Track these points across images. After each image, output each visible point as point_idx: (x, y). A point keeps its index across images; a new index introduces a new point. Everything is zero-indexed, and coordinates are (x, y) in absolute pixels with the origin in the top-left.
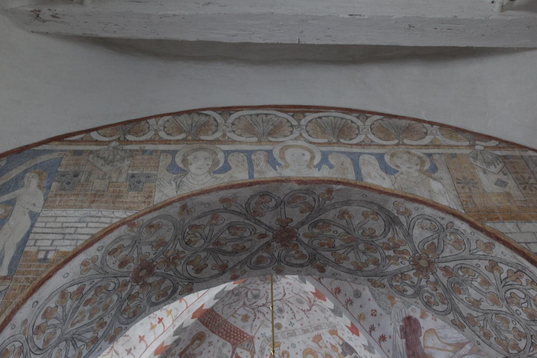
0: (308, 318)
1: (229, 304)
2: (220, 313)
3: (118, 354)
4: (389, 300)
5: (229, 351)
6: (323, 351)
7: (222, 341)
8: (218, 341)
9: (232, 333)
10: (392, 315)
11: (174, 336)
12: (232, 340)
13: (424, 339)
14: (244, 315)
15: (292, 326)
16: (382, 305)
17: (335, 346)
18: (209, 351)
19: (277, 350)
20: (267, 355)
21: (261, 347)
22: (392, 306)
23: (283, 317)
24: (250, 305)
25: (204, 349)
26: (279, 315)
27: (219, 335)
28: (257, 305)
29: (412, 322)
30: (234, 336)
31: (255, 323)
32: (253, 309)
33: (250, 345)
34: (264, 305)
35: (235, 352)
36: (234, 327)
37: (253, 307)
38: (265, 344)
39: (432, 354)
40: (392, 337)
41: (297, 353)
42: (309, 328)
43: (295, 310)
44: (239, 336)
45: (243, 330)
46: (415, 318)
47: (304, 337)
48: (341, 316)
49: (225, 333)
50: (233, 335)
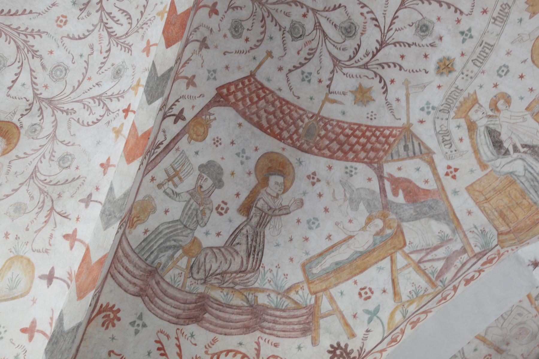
1: (296, 68)
2: (286, 95)
3: (66, 217)
5: (370, 180)
7: (339, 166)
8: (330, 168)
9: (353, 140)
11: (150, 102)
14: (354, 89)
15: (471, 37)
18: (320, 195)
19: (476, 111)
20: (461, 140)
21: (437, 133)
23: (441, 38)
24: (351, 59)
25: (305, 193)
26: (428, 40)
27: (323, 155)
30: (364, 145)
31: (392, 96)
32: (365, 66)
33: (410, 147)
34: (382, 44)
35: (385, 175)
36: (350, 124)
37: (361, 63)
38: (444, 122)
44: (373, 139)
45: (374, 123)
49: (335, 146)
50: (358, 143)
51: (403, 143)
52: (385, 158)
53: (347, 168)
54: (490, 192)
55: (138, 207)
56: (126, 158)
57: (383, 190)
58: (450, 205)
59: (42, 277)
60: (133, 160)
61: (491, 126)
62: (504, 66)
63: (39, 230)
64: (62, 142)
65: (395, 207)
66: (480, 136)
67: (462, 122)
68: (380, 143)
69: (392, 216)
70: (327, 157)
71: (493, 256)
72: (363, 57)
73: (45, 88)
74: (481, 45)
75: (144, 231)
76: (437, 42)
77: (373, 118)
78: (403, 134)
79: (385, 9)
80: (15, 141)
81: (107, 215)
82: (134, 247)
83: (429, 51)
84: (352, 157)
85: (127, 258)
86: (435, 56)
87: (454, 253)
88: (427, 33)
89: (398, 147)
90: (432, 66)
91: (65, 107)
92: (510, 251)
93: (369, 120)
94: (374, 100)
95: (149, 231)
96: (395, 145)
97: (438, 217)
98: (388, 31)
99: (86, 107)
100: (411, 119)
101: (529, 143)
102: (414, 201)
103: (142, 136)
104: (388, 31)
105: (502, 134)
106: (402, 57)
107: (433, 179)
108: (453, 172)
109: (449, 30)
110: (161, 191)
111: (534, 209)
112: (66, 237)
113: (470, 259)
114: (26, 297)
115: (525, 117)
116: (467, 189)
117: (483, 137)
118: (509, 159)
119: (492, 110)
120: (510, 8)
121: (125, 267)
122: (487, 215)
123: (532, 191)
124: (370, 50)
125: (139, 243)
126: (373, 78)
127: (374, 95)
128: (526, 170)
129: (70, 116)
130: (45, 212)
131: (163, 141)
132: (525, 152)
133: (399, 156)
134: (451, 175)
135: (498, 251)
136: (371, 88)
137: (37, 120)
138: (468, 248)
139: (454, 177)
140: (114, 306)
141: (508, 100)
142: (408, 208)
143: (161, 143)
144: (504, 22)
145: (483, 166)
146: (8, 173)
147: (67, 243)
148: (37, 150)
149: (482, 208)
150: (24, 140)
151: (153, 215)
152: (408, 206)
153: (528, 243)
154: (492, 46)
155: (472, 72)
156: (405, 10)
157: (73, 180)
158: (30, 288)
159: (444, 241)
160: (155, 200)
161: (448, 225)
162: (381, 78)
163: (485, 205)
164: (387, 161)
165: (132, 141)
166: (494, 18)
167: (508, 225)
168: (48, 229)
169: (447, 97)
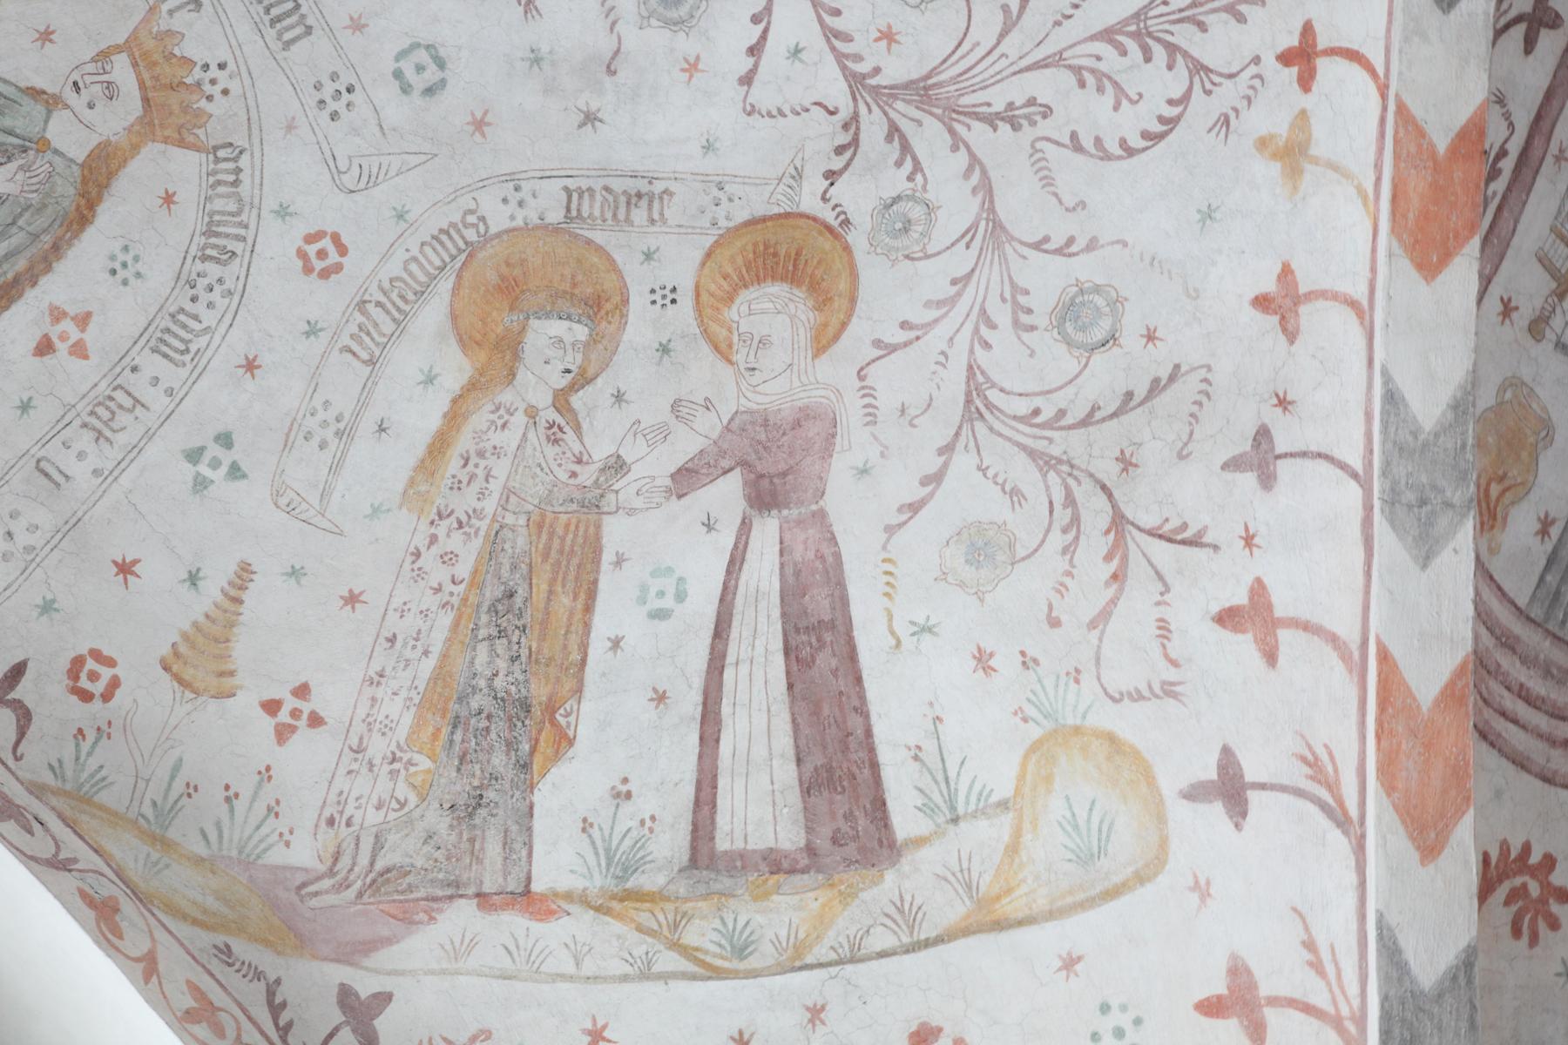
55: (1490, 440)
56: (1412, 260)
59: (1195, 793)
60: (1446, 257)
63: (1104, 615)
64: (1037, 246)
73: (884, 43)
75: (1538, 526)
80: (843, 285)
81: (1410, 507)
82: (1522, 601)
85: (1514, 650)
91: (998, 99)
95: (1553, 522)
99: (1090, 80)
103: (1453, 150)
110: (1547, 346)
112: (1228, 618)
114: (1163, 880)
121: (1516, 688)
125: (1535, 579)
129: (1028, 133)
130: (1095, 543)
131: (1506, 141)
137: (895, 181)
140: (1527, 849)
143: (1503, 153)
146: (871, 418)
147: (1243, 645)
148: (951, 301)
150: (873, 273)
151: (1550, 452)
157: (1156, 387)
158: (1164, 844)
160: (1538, 390)
165: (1418, 184)
168: (1139, 600)
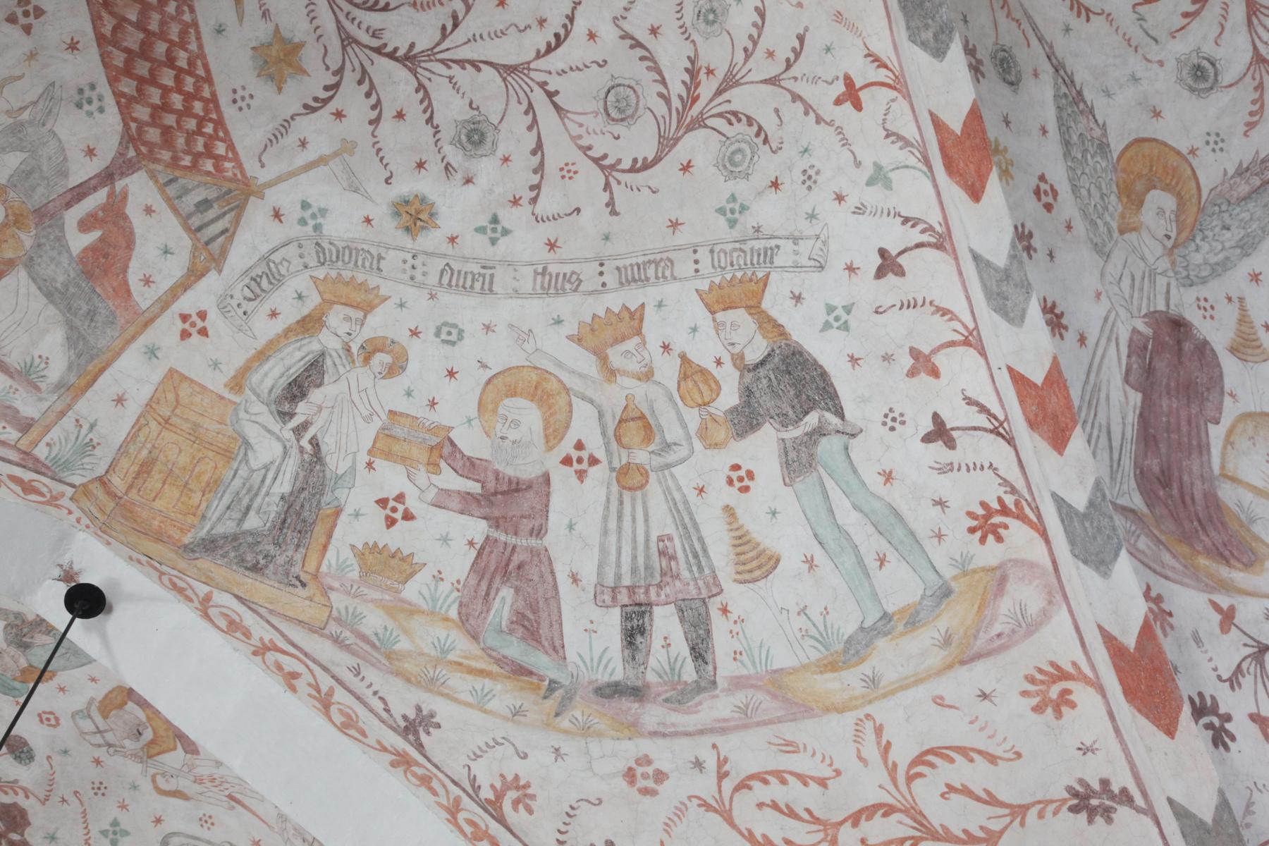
0: (614, 213)
4: (1119, 198)
6: (614, 397)
8: (73, 46)
9: (167, 78)
10: (1110, 268)
12: (142, 112)
13: (1228, 441)
14: (286, 34)
15: (493, 242)
16: (1084, 192)
17: (703, 372)
20: (274, 314)
21: (266, 259)
22: (1122, 232)
23: (468, 181)
26: (455, 156)
27: (96, 20)
28: (375, 34)
29: (1187, 346)
30: (166, 107)
31: (306, 126)
32: (348, 41)
33: (211, 214)
34: (409, 60)
35: (119, 185)
36: (202, 55)
37: (351, 28)
38: (297, 263)
39: (1253, 521)
40: (1091, 342)
41: (451, 374)
42: (589, 272)
43: (559, 151)
44: (191, 124)
45: (228, 111)
46: (1205, 343)
47: (535, 311)
48: (939, 52)
49: (133, 39)
50: (166, 91)
51: (212, 194)
52: (159, 167)
53: (93, 87)
54: (186, 420)
57: (80, 193)
58: (118, 354)
61: (328, 362)
62: (461, 332)
65: (52, 237)
66: (299, 349)
67: (314, 300)
68: (188, 142)
69: (27, 239)
70: (95, 28)
71: (44, 490)
72: (364, 26)
74: (484, 267)
76: (459, 177)
77: (240, 103)
78: (233, 186)
79: (485, 36)
83: (435, 167)
84: (126, 90)
86: (427, 185)
87: (9, 407)
88: (469, 147)
89: (198, 186)
90: (407, 186)
92: (73, 518)
93: (231, 96)
94: (280, 90)
96: (200, 178)
97: (74, 339)
98: (442, 61)
100: (274, 189)
101: (324, 448)
102: (88, 274)
104: (442, 61)
105: (322, 389)
106: (400, 115)
107: (161, 292)
108: (196, 326)
109: (491, 191)
111: (190, 519)
113: (15, 447)
115: (375, 417)
116: (172, 372)
117: (299, 355)
118: (275, 426)
119: (362, 347)
120: (575, 290)
122: (132, 437)
123: (226, 500)
124: (386, 36)
126: (328, 68)
127: (291, 86)
128: (266, 468)
132: (302, 450)
133: (180, 197)
134: (187, 326)
135: (63, 495)
136: (304, 72)
138: (34, 433)
139: (185, 335)
141: (395, 369)
142: (66, 265)
144: (545, 291)
145: (237, 383)
149: (142, 421)
152: (69, 264)
153: (108, 544)
154: (491, 290)
155: (424, 274)
156: (499, 80)
159: (27, 376)
161: (70, 368)
162: (336, 86)
163: (153, 425)
164: (153, 176)
166: (545, 269)
167: (131, 487)
169: (353, 245)
